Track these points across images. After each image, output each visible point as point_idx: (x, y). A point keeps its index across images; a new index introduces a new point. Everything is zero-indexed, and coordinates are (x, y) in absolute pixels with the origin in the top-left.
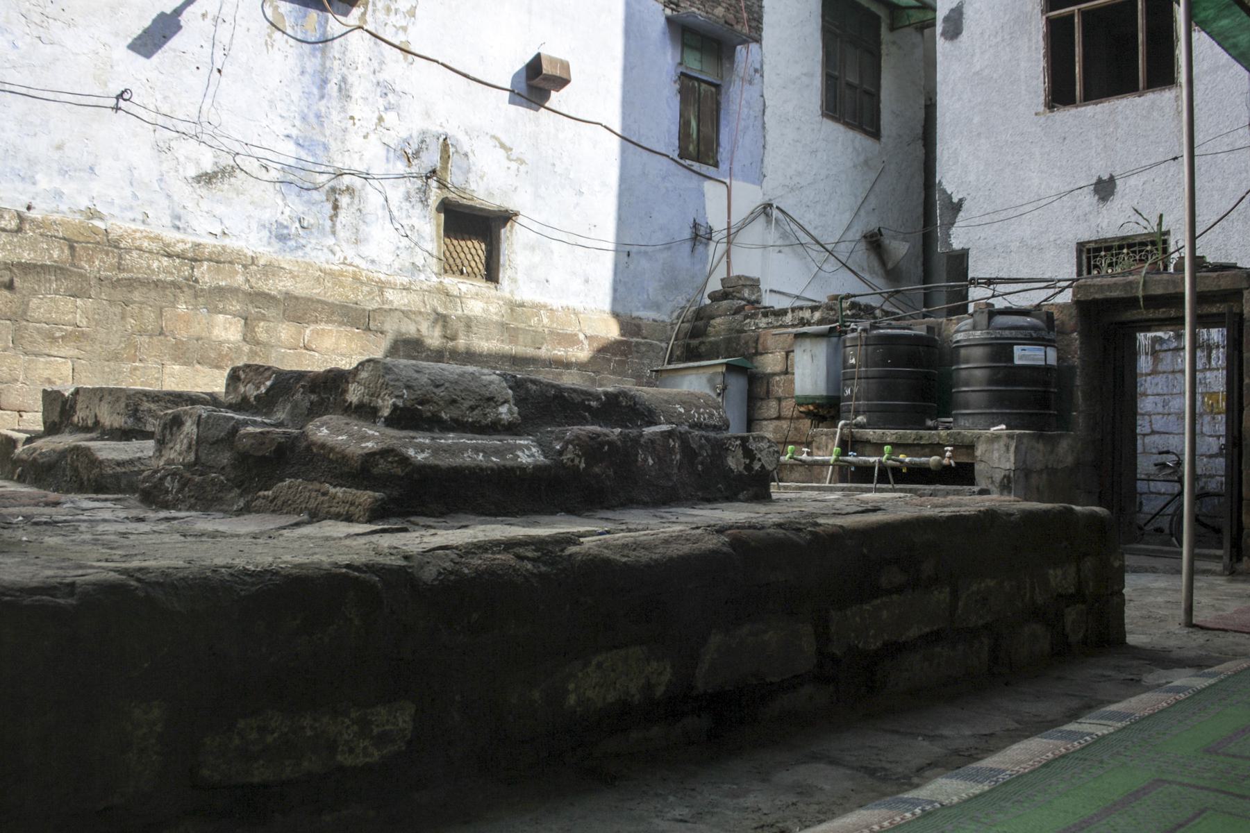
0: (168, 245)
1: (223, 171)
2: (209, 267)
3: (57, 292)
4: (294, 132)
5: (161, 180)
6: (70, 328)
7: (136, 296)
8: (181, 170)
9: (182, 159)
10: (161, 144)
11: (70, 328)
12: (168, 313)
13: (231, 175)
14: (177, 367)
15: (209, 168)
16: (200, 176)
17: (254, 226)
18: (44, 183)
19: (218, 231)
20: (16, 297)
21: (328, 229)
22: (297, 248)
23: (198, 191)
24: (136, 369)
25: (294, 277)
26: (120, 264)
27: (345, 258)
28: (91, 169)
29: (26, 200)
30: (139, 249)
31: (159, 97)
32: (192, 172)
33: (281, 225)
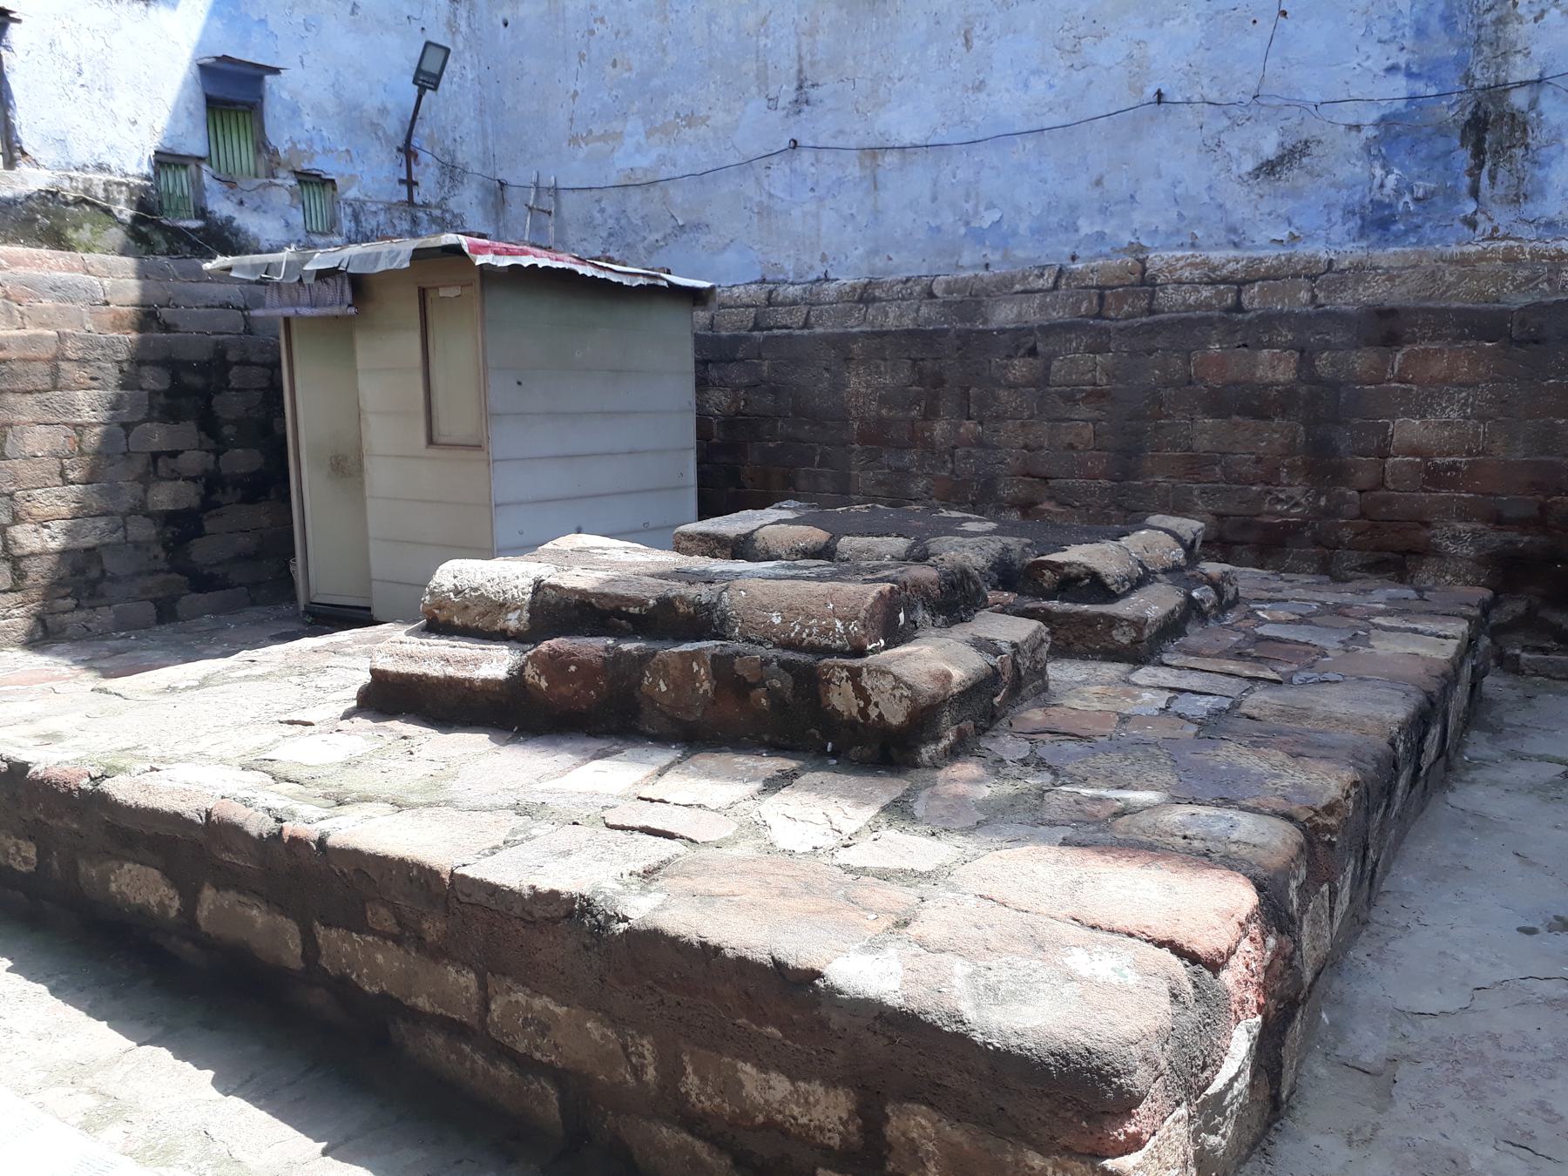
0: (1214, 269)
1: (1292, 152)
2: (1261, 288)
3: (1076, 351)
4: (1402, 59)
5: (1210, 188)
6: (1088, 388)
7: (1159, 342)
8: (1234, 168)
9: (1235, 152)
10: (1209, 142)
11: (1088, 388)
12: (1197, 356)
13: (1303, 154)
14: (1209, 421)
15: (1270, 149)
16: (1259, 169)
17: (1337, 215)
18: (1086, 228)
19: (1283, 235)
20: (1037, 362)
21: (1465, 190)
22: (1406, 233)
23: (1257, 190)
24: (1162, 427)
25: (1389, 279)
26: (1150, 304)
27: (1495, 229)
28: (1132, 197)
29: (1068, 250)
30: (1180, 282)
31: (1205, 81)
32: (1249, 165)
33: (1378, 205)
